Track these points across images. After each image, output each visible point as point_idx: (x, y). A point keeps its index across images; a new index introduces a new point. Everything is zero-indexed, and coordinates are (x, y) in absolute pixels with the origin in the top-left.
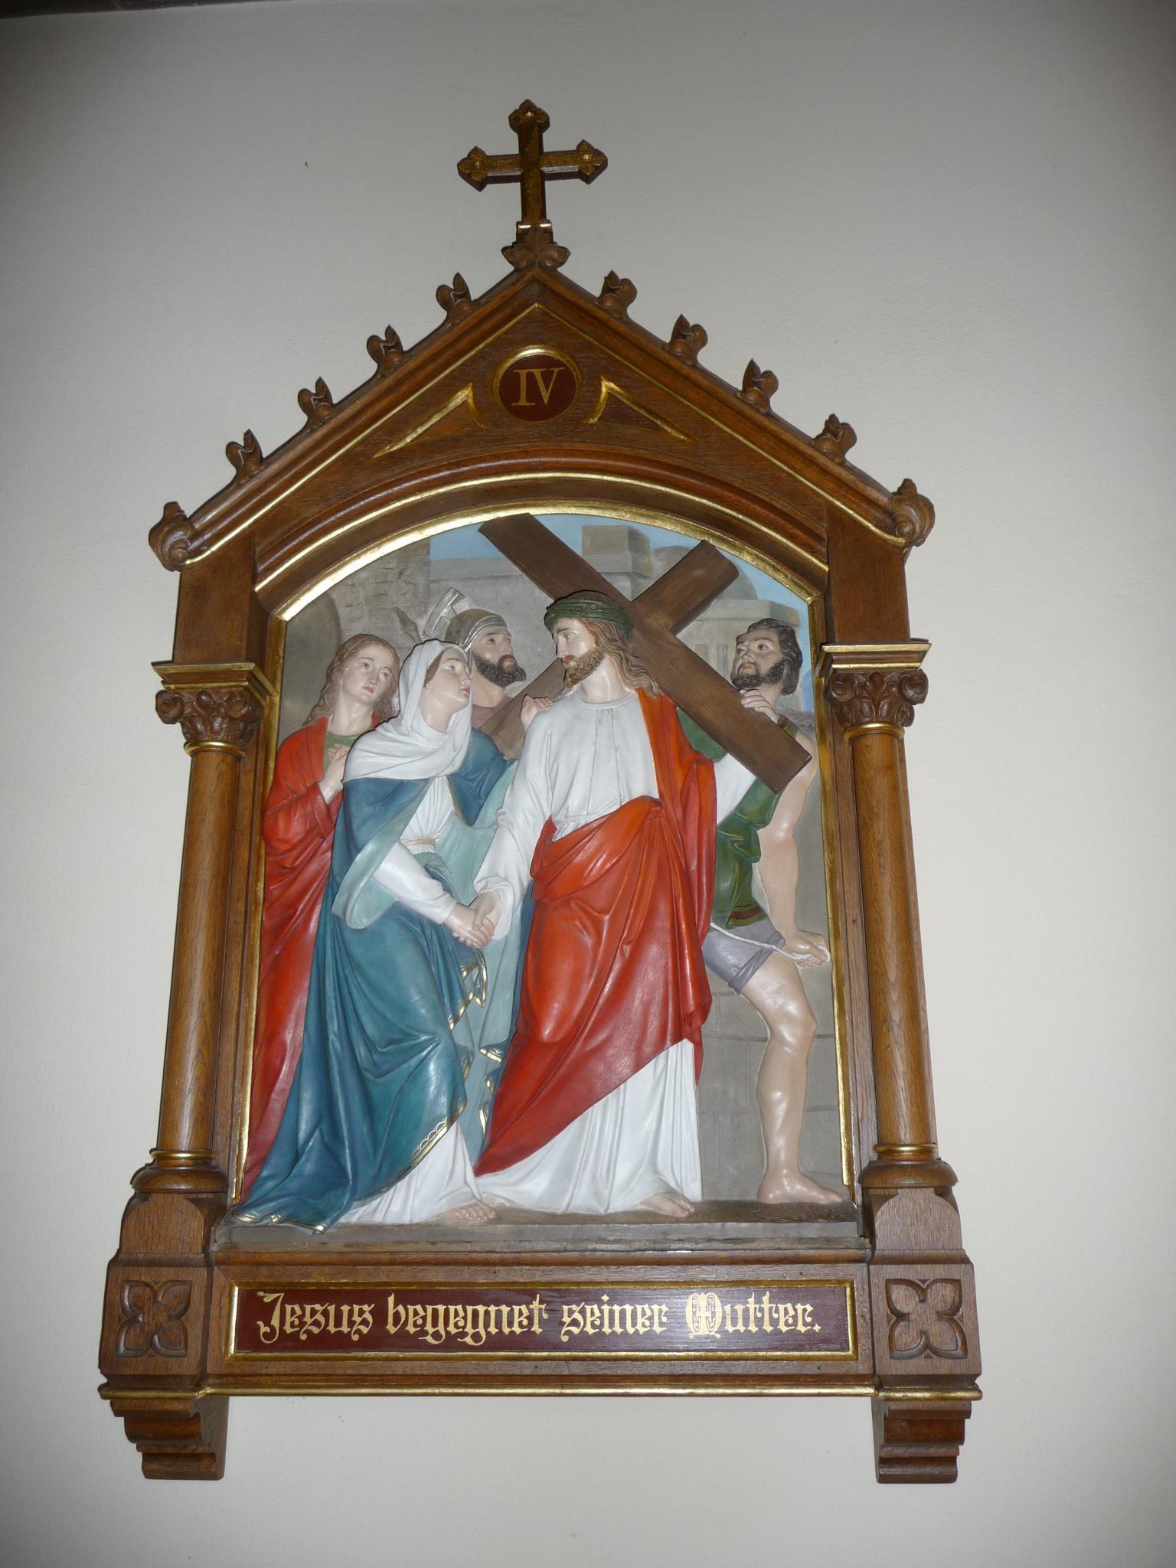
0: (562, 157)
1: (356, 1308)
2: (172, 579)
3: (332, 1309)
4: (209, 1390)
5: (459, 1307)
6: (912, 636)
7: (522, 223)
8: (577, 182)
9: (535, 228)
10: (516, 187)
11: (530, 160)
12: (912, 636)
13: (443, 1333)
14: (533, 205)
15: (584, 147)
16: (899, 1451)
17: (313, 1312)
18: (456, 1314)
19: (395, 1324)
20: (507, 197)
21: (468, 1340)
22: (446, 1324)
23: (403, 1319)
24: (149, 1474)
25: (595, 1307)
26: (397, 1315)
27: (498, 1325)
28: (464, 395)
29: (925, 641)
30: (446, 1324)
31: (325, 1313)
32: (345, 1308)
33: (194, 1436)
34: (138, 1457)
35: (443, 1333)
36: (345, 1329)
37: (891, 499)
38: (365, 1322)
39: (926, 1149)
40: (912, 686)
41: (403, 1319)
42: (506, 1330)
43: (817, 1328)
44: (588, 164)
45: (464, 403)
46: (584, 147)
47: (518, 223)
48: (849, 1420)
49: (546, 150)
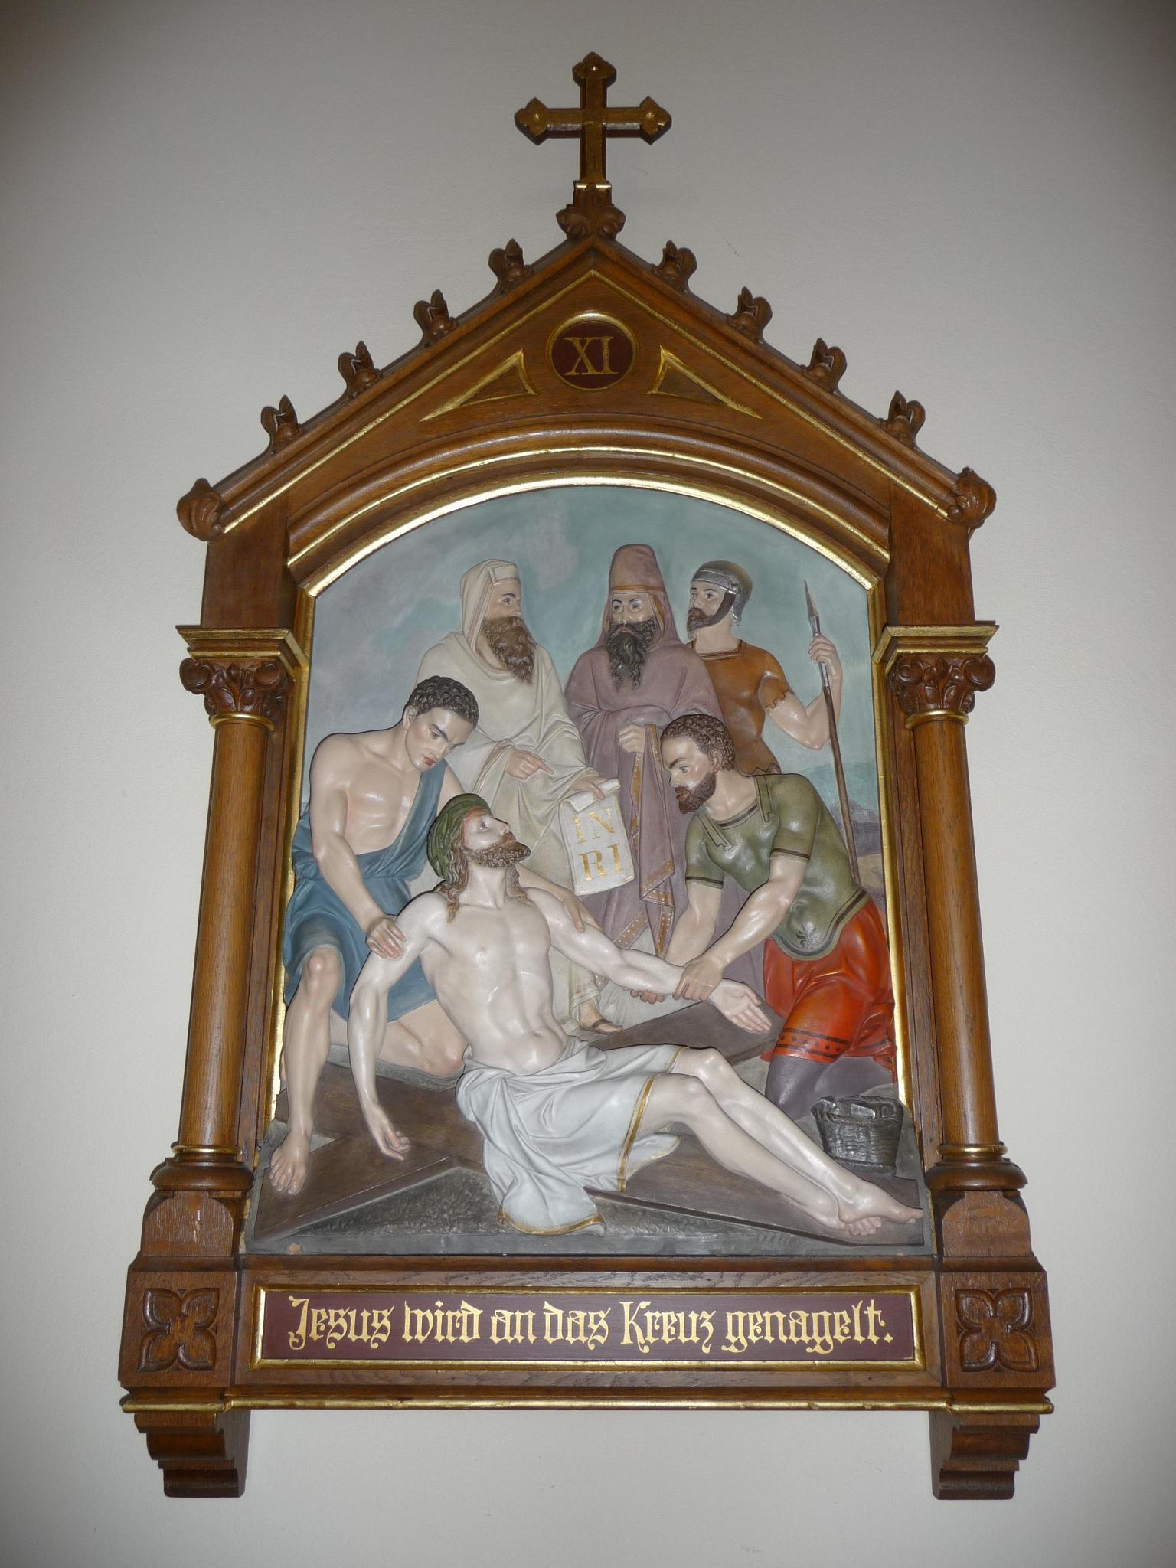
0: (624, 113)
1: (376, 1313)
2: (201, 547)
3: (353, 1314)
4: (233, 1403)
6: (977, 618)
7: (580, 182)
8: (639, 141)
9: (592, 189)
10: (575, 143)
11: (593, 115)
12: (977, 618)
13: (830, 1342)
14: (592, 163)
15: (649, 104)
17: (337, 1316)
18: (842, 1321)
20: (566, 152)
21: (818, 1349)
22: (832, 1333)
25: (844, 1313)
27: (774, 1333)
28: (517, 357)
29: (992, 624)
30: (832, 1333)
31: (347, 1318)
32: (365, 1314)
33: (221, 1451)
34: (160, 1474)
35: (830, 1342)
36: (365, 1337)
37: (957, 482)
39: (993, 1153)
40: (983, 673)
42: (783, 1339)
43: (888, 1338)
44: (651, 123)
45: (513, 370)
46: (649, 104)
47: (575, 183)
48: (906, 1436)
49: (609, 105)
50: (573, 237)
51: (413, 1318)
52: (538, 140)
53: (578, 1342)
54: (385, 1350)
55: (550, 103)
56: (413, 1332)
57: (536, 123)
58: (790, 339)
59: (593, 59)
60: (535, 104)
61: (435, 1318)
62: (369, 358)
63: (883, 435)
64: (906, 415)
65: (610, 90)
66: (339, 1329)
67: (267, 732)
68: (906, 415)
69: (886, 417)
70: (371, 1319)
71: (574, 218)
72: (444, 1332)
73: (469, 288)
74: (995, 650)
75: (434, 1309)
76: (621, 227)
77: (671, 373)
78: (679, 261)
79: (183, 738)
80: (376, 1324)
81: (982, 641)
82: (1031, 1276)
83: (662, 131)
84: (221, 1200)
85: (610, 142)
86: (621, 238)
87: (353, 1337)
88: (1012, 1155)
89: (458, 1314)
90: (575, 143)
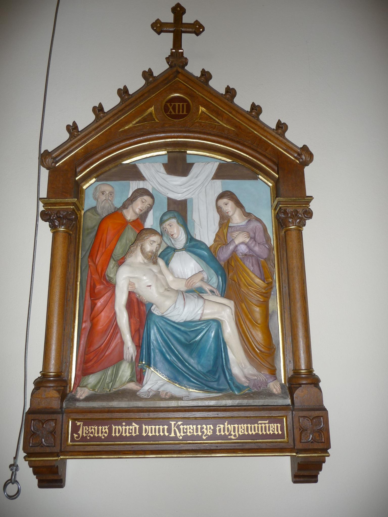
0: (188, 25)
5: (273, 425)
8: (194, 35)
10: (171, 35)
11: (178, 26)
15: (197, 22)
19: (145, 433)
20: (168, 38)
23: (121, 431)
24: (40, 486)
26: (228, 428)
36: (100, 435)
38: (106, 432)
41: (121, 431)
44: (197, 29)
50: (171, 66)
51: (115, 429)
52: (159, 33)
54: (106, 439)
55: (163, 21)
56: (115, 433)
57: (158, 27)
58: (243, 102)
60: (158, 21)
61: (122, 429)
63: (274, 134)
64: (282, 127)
65: (184, 17)
68: (282, 127)
70: (102, 429)
71: (171, 59)
72: (125, 433)
75: (122, 426)
77: (203, 112)
80: (104, 431)
83: (201, 32)
85: (183, 34)
86: (186, 68)
87: (96, 435)
89: (131, 427)
90: (171, 35)
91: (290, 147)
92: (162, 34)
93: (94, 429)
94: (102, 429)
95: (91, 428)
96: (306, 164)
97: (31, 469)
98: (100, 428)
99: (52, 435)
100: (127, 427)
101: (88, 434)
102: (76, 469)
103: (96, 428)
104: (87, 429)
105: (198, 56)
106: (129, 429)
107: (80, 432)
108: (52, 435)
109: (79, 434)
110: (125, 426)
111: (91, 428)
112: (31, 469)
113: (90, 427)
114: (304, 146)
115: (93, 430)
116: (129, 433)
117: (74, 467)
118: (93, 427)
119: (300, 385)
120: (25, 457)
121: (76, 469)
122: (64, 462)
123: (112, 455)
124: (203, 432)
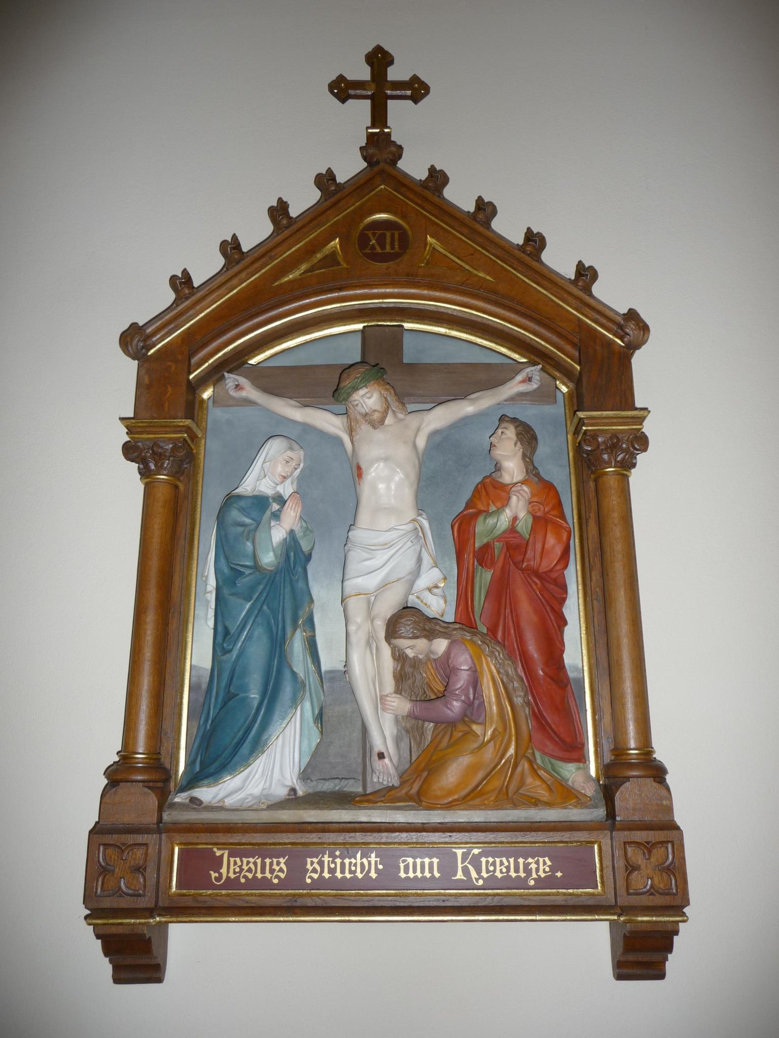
10: (368, 102)
11: (379, 85)
15: (415, 79)
16: (631, 957)
29: (646, 409)
52: (343, 101)
53: (264, 878)
55: (350, 77)
57: (342, 89)
58: (509, 227)
59: (379, 49)
62: (239, 245)
64: (586, 274)
66: (249, 870)
67: (177, 487)
68: (586, 274)
69: (573, 278)
71: (371, 151)
73: (303, 198)
74: (648, 428)
76: (400, 157)
78: (437, 178)
79: (122, 493)
81: (641, 420)
82: (671, 834)
84: (149, 788)
86: (401, 164)
88: (659, 755)
91: (601, 312)
92: (350, 102)
93: (255, 864)
94: (271, 864)
95: (248, 863)
96: (633, 347)
97: (100, 941)
98: (268, 861)
99: (150, 877)
100: (347, 861)
101: (240, 872)
102: (186, 942)
103: (259, 861)
104: (239, 863)
105: (423, 141)
106: (350, 863)
107: (224, 871)
108: (150, 877)
109: (221, 875)
110: (342, 857)
111: (248, 863)
112: (100, 941)
113: (245, 860)
114: (630, 310)
115: (252, 865)
116: (351, 872)
117: (184, 940)
118: (251, 860)
119: (628, 778)
120: (86, 917)
121: (186, 942)
122: (163, 929)
123: (309, 916)
124: (272, 871)
